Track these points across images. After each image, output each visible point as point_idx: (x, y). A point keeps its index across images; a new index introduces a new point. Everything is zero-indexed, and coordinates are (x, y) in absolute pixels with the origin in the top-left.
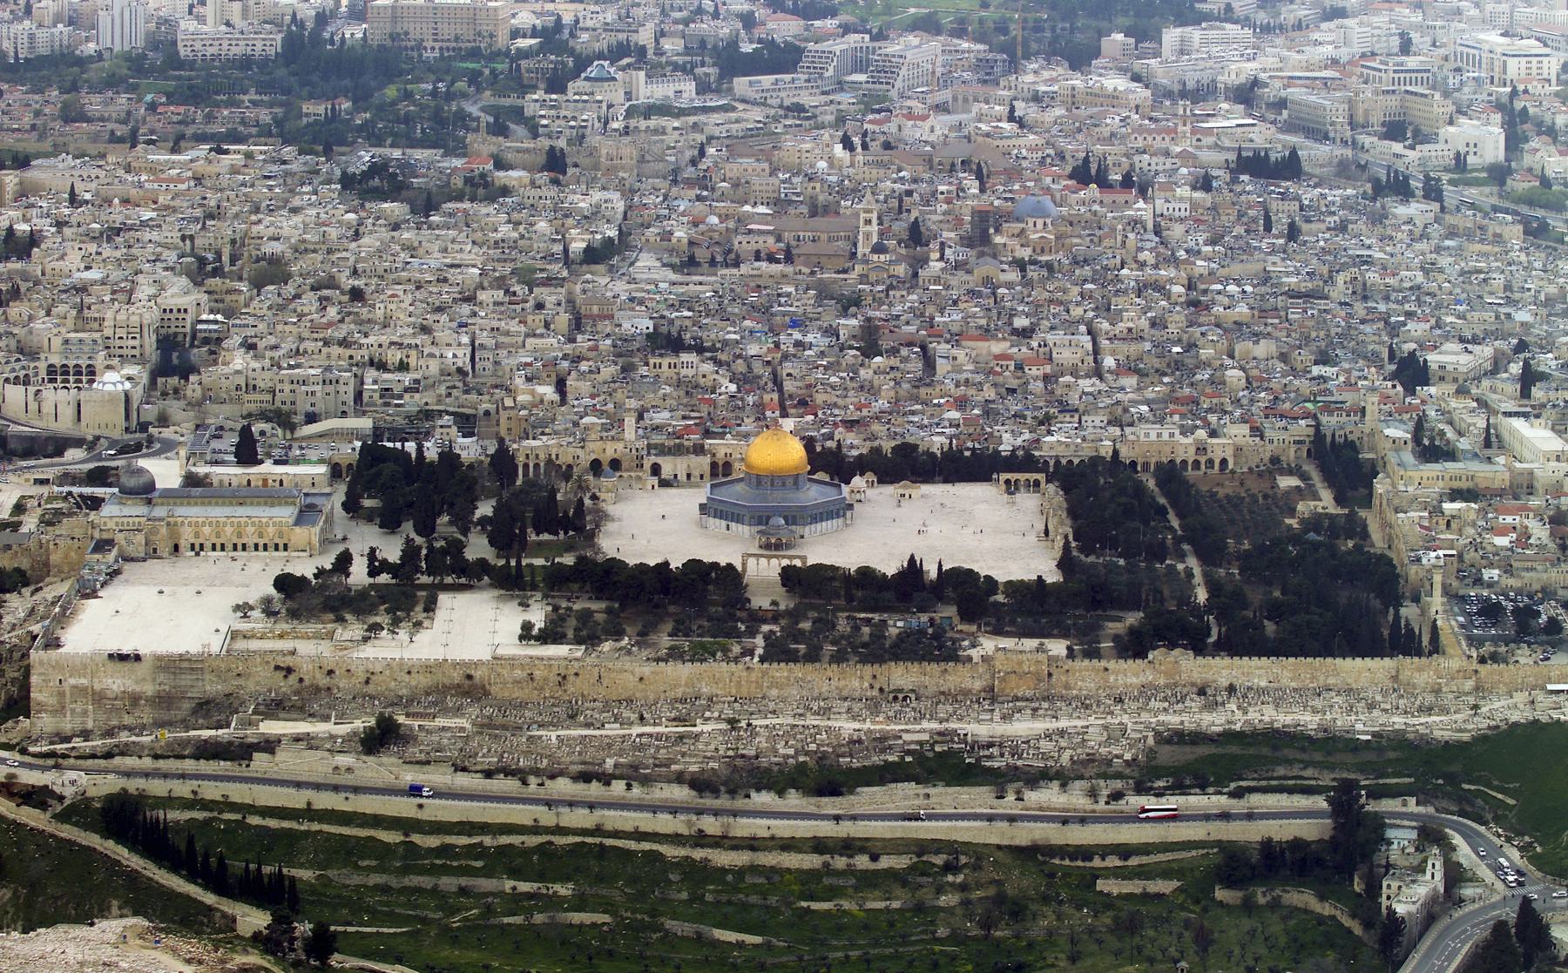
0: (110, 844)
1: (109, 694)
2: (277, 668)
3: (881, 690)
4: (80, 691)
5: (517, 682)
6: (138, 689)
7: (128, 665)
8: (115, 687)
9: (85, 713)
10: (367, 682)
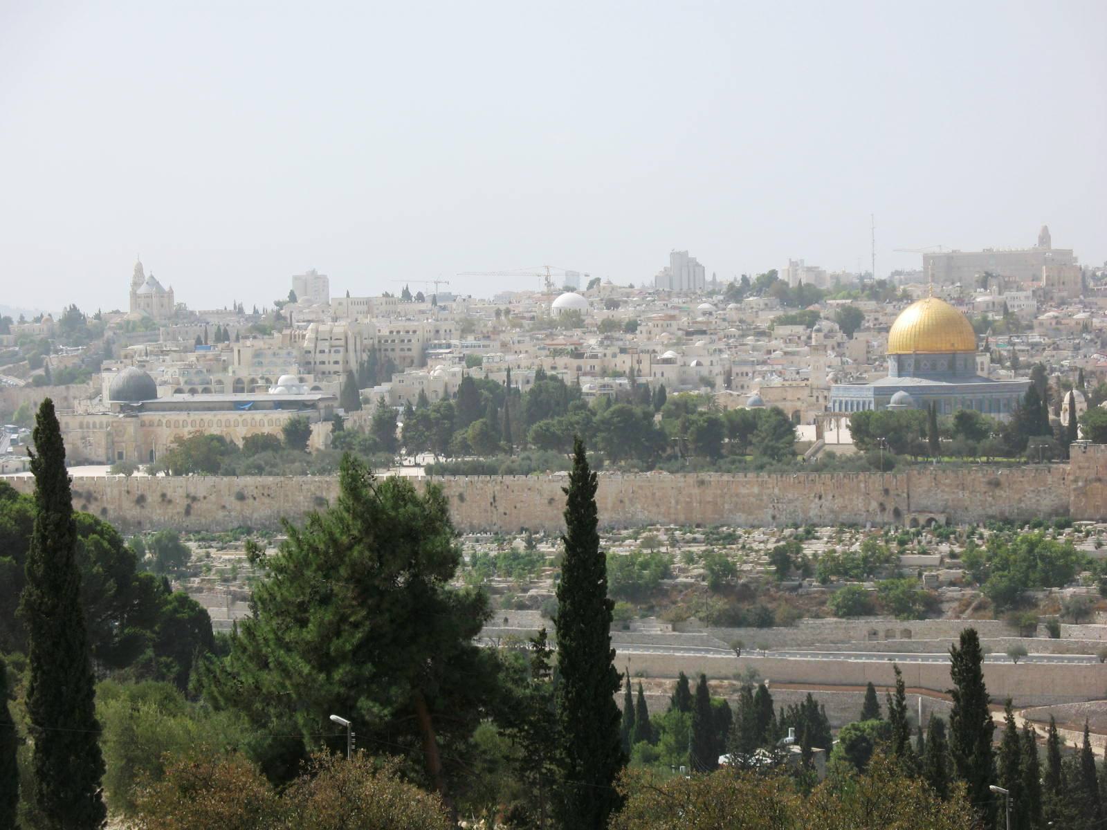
10: (188, 512)
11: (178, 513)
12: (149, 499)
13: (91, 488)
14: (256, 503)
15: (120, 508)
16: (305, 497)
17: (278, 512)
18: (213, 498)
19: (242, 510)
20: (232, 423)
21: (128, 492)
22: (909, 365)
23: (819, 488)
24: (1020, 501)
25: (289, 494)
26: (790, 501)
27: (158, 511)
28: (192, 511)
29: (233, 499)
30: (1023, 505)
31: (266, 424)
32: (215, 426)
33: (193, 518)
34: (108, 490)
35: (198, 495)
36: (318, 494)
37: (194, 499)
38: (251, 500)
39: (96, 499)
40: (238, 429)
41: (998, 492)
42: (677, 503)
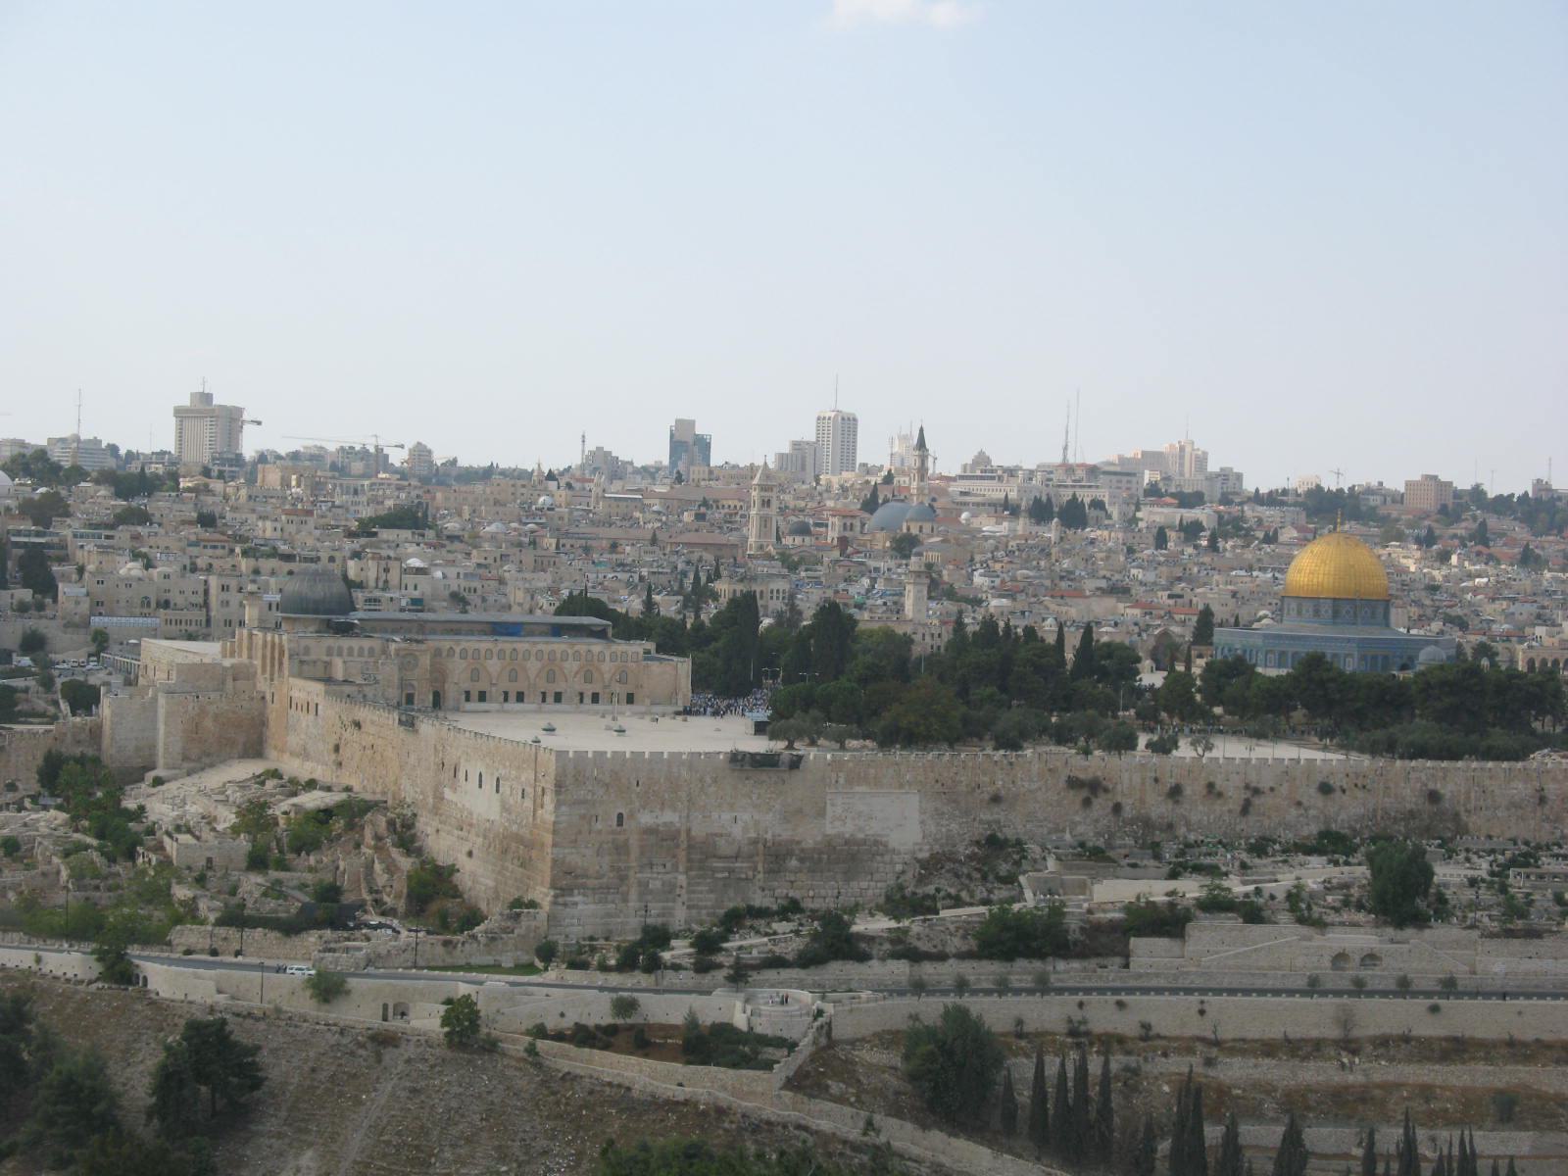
0: (937, 1137)
2: (1074, 783)
4: (663, 840)
5: (1514, 805)
6: (785, 833)
7: (766, 776)
8: (737, 831)
9: (670, 889)
10: (1245, 809)
11: (1230, 811)
12: (1188, 791)
13: (1099, 774)
14: (1345, 798)
15: (1142, 801)
17: (1375, 810)
18: (1284, 789)
20: (558, 655)
21: (1156, 780)
22: (1307, 611)
25: (1392, 785)
27: (1201, 808)
28: (1251, 809)
29: (1313, 791)
31: (608, 658)
32: (533, 658)
33: (1252, 819)
34: (1126, 776)
35: (1260, 786)
36: (1431, 786)
37: (1257, 791)
38: (1338, 793)
39: (1106, 790)
40: (566, 665)
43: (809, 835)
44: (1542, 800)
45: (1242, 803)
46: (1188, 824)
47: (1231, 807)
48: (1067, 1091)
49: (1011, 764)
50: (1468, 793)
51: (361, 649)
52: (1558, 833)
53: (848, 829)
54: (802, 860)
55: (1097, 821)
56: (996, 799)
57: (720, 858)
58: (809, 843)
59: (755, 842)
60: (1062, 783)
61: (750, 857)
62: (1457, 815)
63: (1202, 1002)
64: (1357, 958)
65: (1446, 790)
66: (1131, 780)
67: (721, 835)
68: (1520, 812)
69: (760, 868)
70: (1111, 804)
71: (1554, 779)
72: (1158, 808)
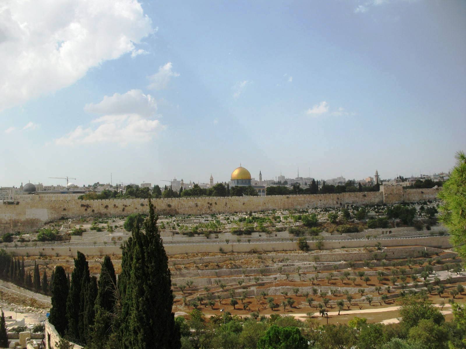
1: (3, 221)
2: (83, 206)
3: (341, 204)
7: (12, 206)
8: (6, 218)
10: (123, 210)
11: (120, 211)
12: (110, 207)
13: (89, 204)
15: (99, 209)
16: (164, 205)
18: (133, 205)
19: (143, 209)
21: (102, 204)
23: (320, 198)
24: (371, 200)
26: (313, 202)
27: (113, 210)
28: (125, 210)
29: (139, 206)
30: (371, 201)
33: (125, 212)
34: (95, 204)
36: (169, 203)
37: (126, 206)
38: (146, 206)
39: (90, 207)
41: (365, 198)
42: (281, 203)
43: (23, 218)
44: (197, 206)
45: (122, 209)
46: (110, 213)
47: (120, 210)
48: (13, 267)
49: (68, 202)
50: (178, 205)
51: (25, 197)
52: (201, 213)
53: (31, 217)
54: (21, 223)
55: (89, 214)
56: (65, 209)
57: (3, 224)
58: (23, 220)
59: (10, 220)
60: (80, 206)
61: (9, 223)
62: (176, 210)
63: (70, 248)
64: (117, 238)
65: (173, 204)
66: (96, 204)
67: (3, 219)
68: (192, 209)
69: (12, 225)
70: (92, 210)
71: (200, 201)
72: (103, 211)
